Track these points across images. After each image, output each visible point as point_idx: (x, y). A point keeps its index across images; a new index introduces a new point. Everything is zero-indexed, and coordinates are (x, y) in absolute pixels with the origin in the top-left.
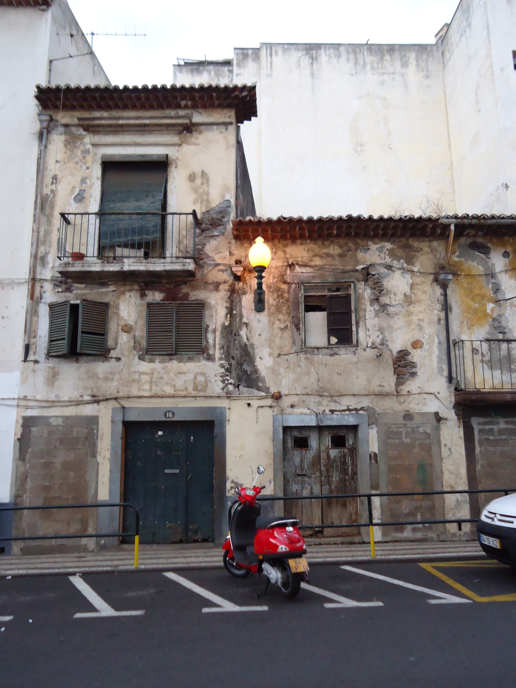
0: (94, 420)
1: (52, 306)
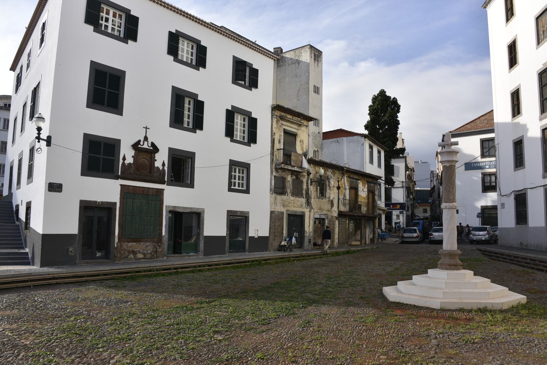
0: (283, 213)
1: (275, 176)
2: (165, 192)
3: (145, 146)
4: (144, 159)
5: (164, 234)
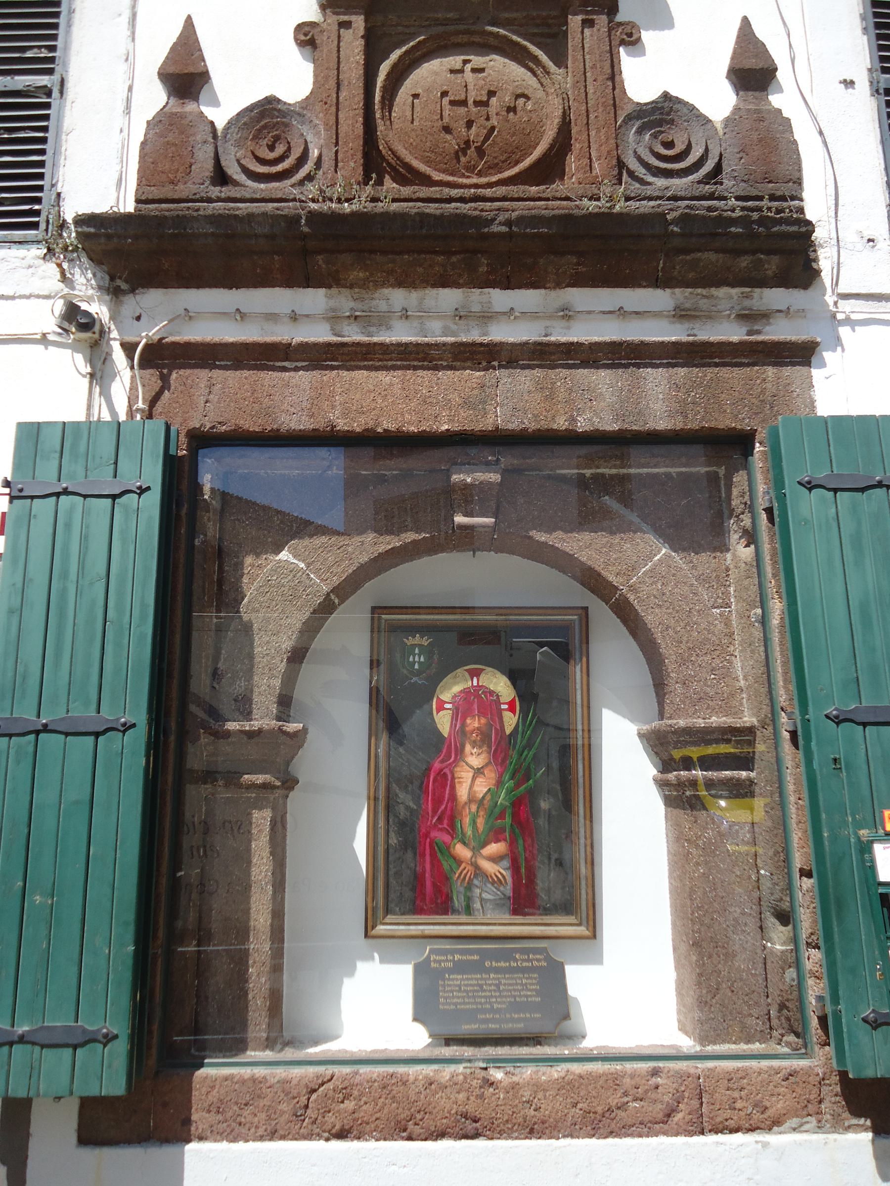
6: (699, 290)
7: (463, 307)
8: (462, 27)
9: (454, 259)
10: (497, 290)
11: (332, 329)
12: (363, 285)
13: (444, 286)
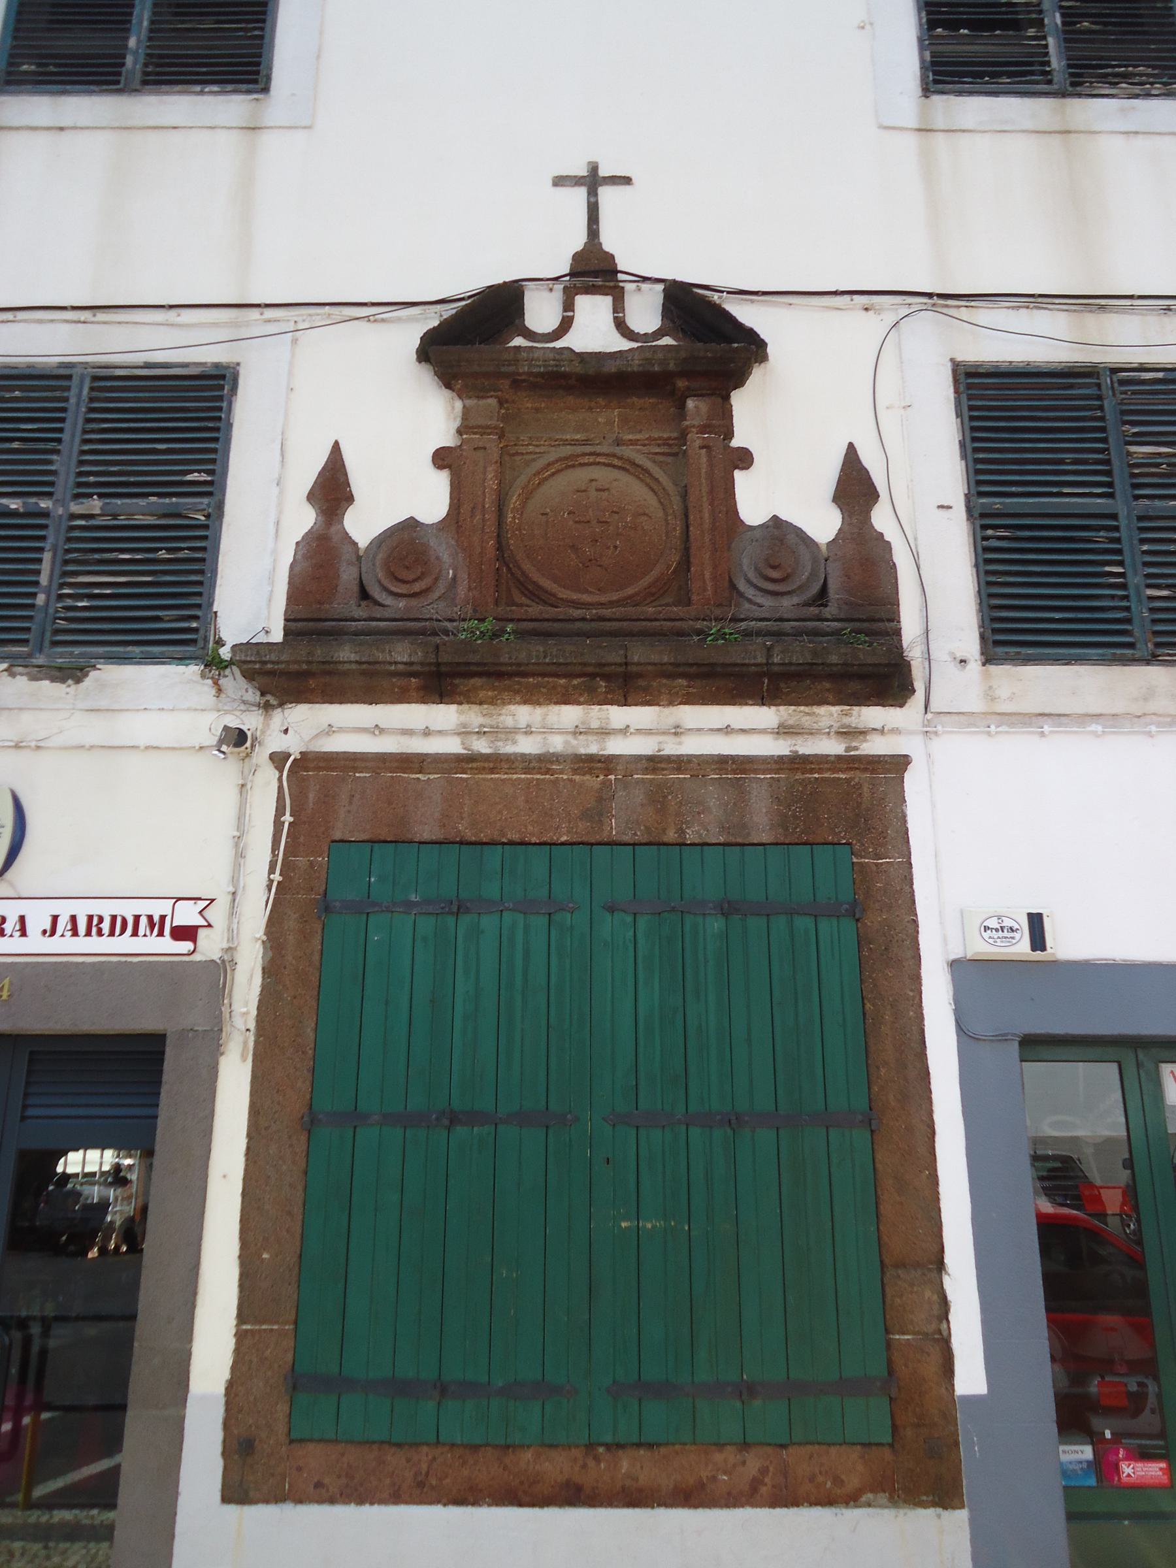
2: (913, 783)
3: (593, 330)
4: (597, 477)
5: (970, 1377)
6: (802, 708)
7: (583, 723)
8: (588, 449)
9: (575, 682)
10: (615, 707)
11: (463, 744)
12: (492, 702)
13: (566, 702)
